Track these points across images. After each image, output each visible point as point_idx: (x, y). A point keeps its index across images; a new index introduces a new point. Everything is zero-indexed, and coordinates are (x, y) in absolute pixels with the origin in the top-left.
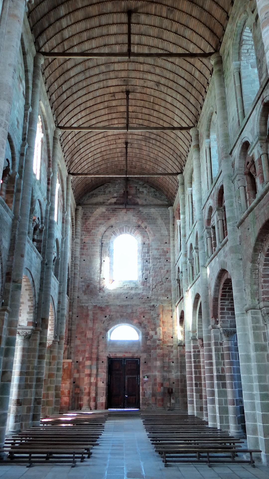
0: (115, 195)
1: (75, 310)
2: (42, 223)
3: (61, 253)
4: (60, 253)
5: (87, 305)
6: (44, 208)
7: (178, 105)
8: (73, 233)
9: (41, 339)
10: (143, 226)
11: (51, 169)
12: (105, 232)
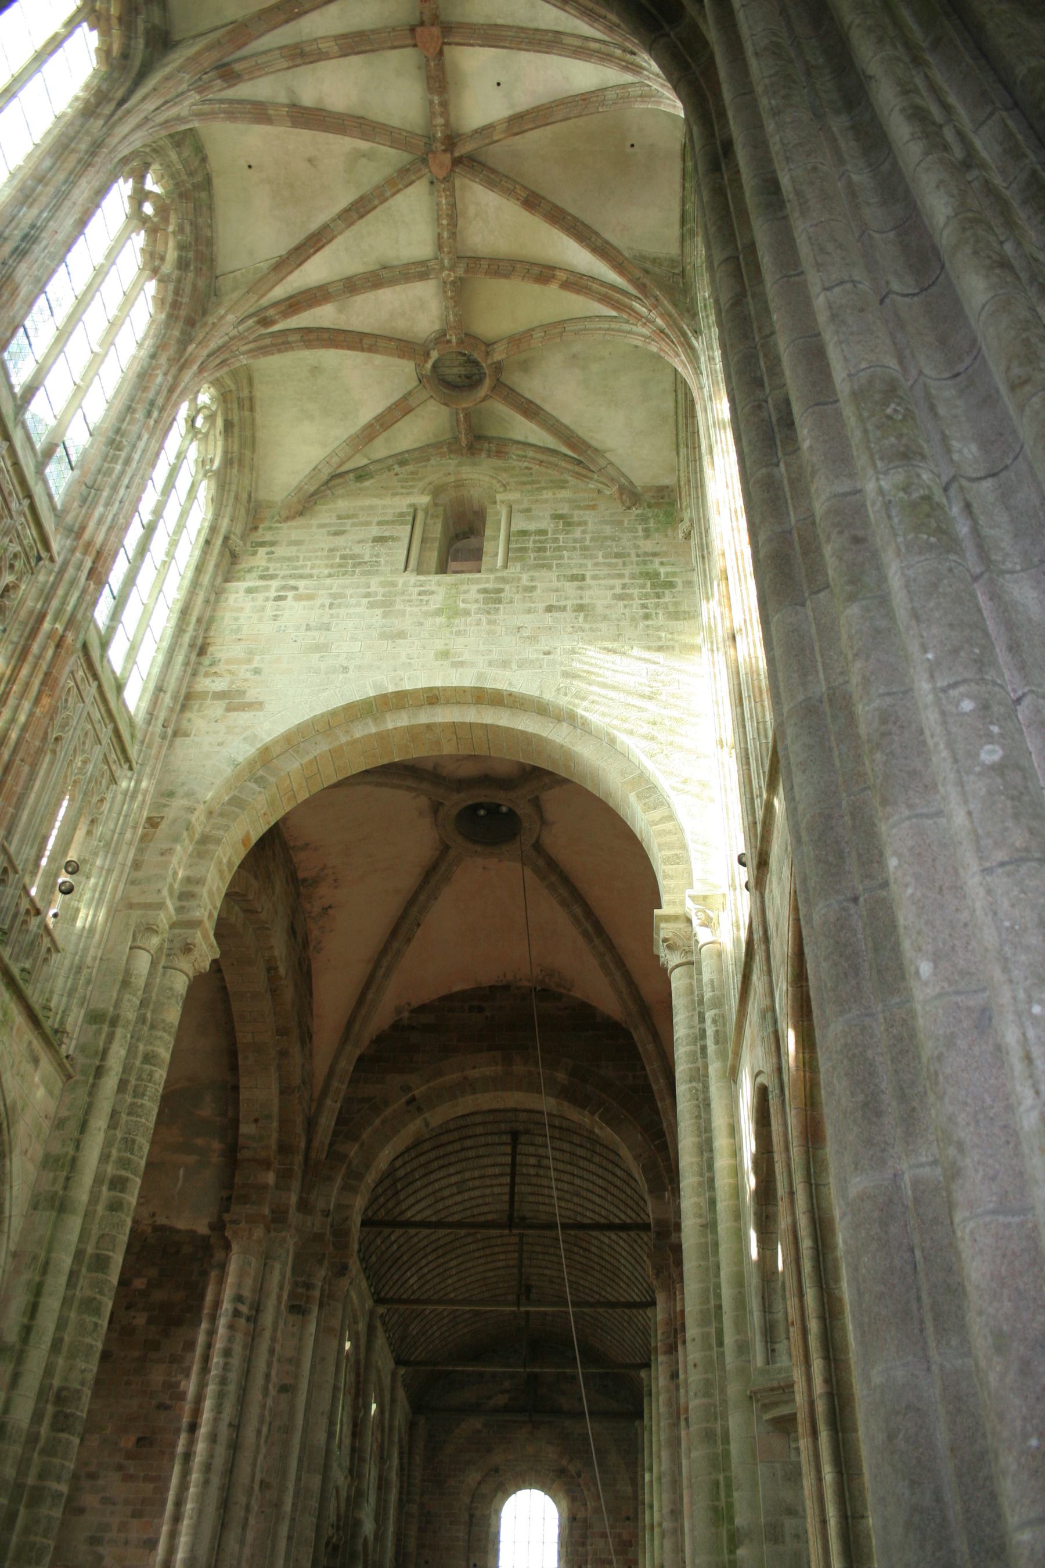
0: (507, 1384)
7: (624, 1253)
10: (572, 1469)
11: (361, 1401)
12: (480, 1483)
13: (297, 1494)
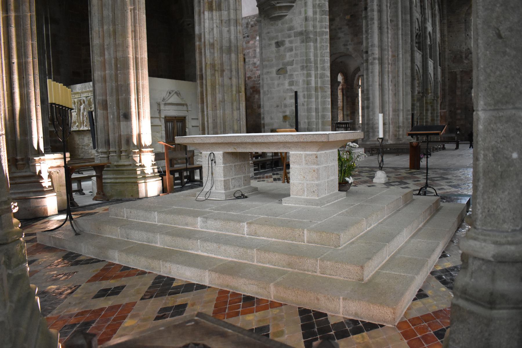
1: (447, 75)
2: (420, 30)
3: (434, 40)
4: (432, 41)
5: (455, 70)
6: (420, 20)
8: (440, 16)
9: (426, 100)
13: (402, 21)
